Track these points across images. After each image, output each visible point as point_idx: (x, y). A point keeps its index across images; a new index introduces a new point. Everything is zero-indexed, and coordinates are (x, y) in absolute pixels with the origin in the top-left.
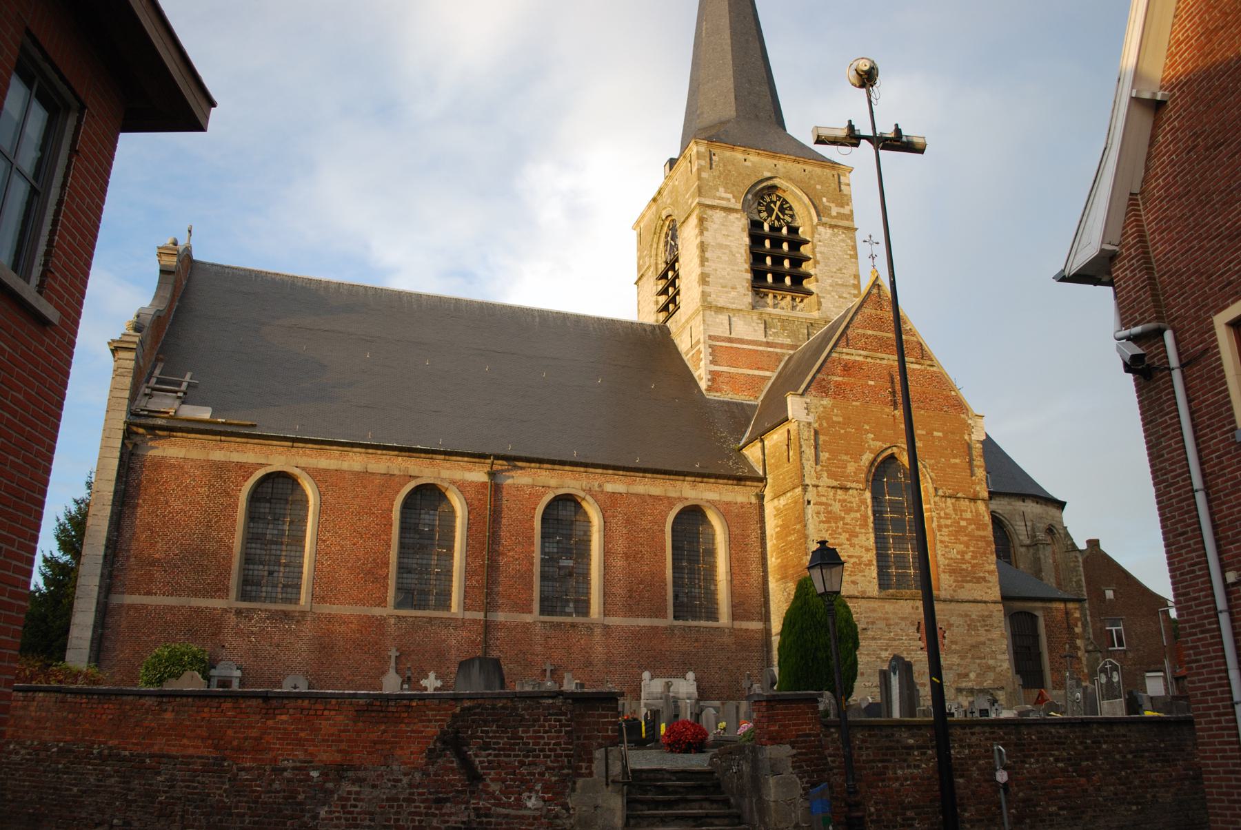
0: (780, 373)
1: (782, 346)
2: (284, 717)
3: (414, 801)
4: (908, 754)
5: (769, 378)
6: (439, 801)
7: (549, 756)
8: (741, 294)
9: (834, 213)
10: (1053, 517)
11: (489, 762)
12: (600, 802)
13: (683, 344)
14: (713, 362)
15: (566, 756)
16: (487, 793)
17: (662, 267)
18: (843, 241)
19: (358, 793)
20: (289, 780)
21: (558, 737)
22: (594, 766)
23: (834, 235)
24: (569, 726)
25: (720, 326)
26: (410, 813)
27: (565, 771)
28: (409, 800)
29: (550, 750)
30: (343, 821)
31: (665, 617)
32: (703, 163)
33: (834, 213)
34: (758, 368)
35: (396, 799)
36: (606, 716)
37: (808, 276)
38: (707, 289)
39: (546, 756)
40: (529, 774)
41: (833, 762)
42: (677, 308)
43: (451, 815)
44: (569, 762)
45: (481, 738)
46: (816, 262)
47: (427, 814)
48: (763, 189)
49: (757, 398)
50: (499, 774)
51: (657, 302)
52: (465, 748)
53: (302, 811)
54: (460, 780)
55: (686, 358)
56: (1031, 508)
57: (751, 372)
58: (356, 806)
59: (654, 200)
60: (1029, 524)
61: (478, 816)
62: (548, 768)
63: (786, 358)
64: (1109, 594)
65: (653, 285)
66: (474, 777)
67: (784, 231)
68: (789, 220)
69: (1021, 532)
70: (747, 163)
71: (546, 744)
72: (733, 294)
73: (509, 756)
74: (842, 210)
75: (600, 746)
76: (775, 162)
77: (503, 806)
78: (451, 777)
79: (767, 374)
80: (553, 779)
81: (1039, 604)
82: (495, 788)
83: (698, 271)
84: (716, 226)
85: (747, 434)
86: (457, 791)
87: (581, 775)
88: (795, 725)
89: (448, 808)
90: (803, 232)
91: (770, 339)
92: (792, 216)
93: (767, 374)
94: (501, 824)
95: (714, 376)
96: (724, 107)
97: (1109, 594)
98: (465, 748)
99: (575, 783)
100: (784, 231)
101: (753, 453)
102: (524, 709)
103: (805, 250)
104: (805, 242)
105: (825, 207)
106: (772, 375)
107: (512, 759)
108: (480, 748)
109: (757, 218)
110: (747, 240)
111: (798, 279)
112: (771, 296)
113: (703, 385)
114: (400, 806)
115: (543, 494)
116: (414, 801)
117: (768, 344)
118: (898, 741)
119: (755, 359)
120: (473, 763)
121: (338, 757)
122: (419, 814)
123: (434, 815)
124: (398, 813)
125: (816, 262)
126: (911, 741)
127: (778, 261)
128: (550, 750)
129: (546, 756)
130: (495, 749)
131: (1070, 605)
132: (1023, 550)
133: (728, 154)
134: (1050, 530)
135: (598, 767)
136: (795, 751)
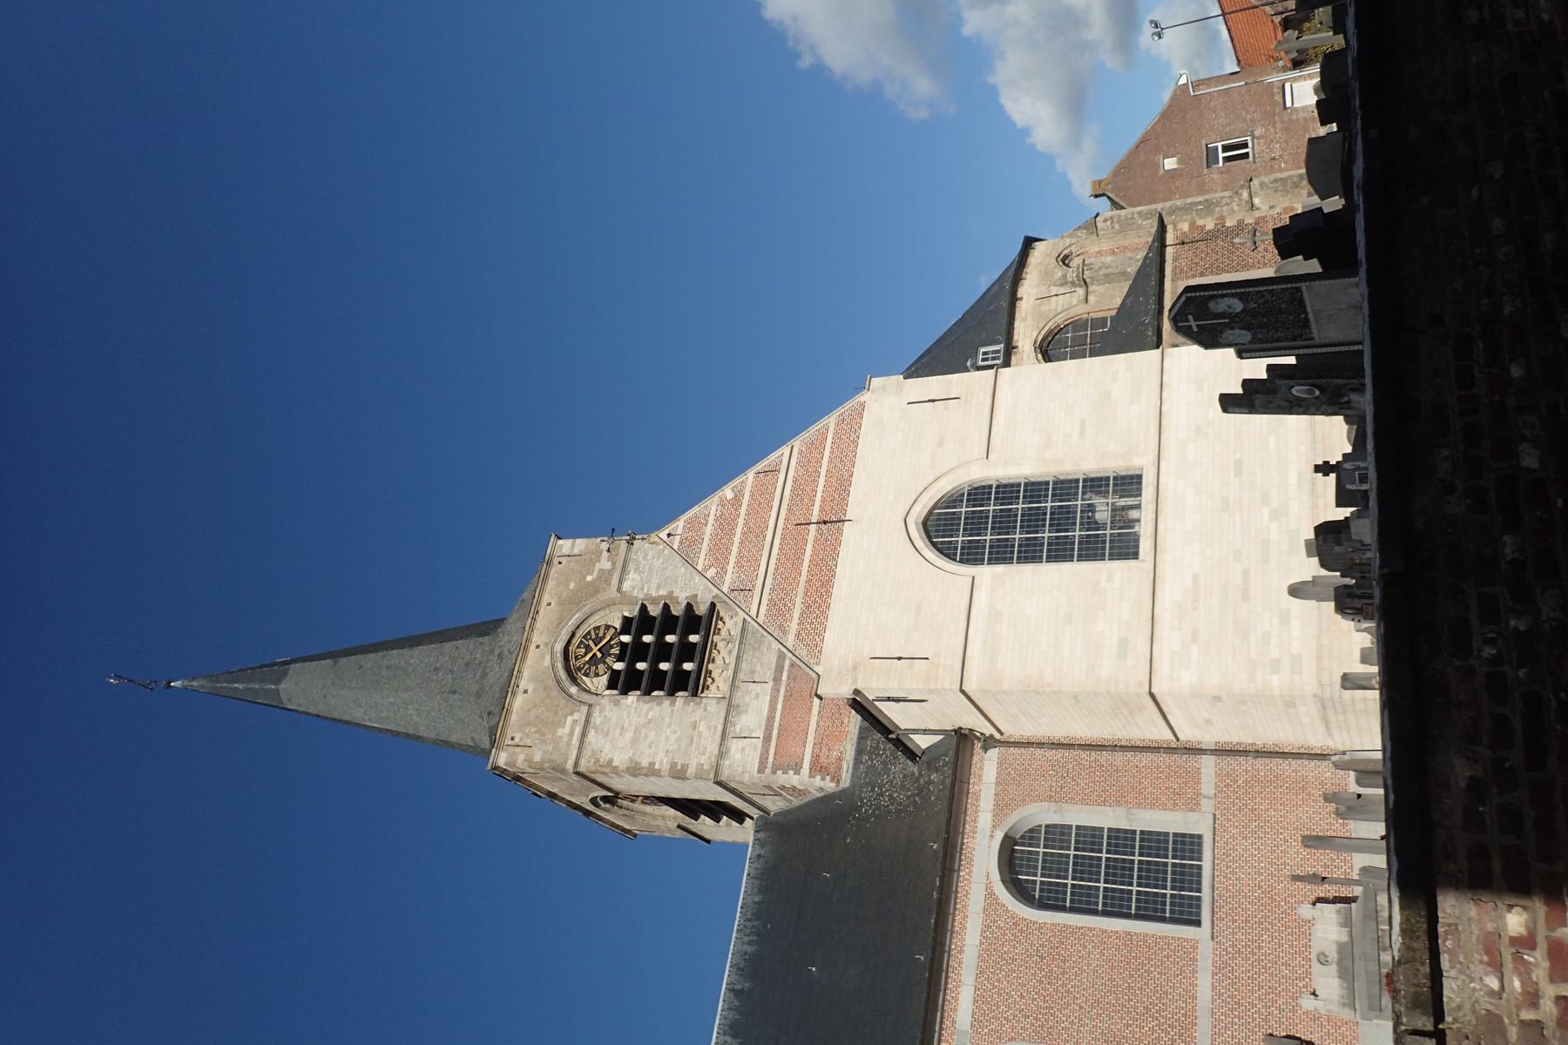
9: (608, 566)
33: (608, 566)
37: (689, 607)
60: (1054, 290)
64: (1170, 163)
67: (626, 639)
68: (612, 631)
72: (702, 727)
76: (532, 647)
90: (634, 612)
91: (769, 675)
92: (608, 627)
95: (818, 768)
97: (1170, 163)
100: (626, 639)
103: (654, 611)
104: (644, 608)
105: (599, 577)
110: (633, 697)
112: (711, 667)
113: (830, 786)
117: (777, 680)
127: (663, 651)
133: (514, 717)
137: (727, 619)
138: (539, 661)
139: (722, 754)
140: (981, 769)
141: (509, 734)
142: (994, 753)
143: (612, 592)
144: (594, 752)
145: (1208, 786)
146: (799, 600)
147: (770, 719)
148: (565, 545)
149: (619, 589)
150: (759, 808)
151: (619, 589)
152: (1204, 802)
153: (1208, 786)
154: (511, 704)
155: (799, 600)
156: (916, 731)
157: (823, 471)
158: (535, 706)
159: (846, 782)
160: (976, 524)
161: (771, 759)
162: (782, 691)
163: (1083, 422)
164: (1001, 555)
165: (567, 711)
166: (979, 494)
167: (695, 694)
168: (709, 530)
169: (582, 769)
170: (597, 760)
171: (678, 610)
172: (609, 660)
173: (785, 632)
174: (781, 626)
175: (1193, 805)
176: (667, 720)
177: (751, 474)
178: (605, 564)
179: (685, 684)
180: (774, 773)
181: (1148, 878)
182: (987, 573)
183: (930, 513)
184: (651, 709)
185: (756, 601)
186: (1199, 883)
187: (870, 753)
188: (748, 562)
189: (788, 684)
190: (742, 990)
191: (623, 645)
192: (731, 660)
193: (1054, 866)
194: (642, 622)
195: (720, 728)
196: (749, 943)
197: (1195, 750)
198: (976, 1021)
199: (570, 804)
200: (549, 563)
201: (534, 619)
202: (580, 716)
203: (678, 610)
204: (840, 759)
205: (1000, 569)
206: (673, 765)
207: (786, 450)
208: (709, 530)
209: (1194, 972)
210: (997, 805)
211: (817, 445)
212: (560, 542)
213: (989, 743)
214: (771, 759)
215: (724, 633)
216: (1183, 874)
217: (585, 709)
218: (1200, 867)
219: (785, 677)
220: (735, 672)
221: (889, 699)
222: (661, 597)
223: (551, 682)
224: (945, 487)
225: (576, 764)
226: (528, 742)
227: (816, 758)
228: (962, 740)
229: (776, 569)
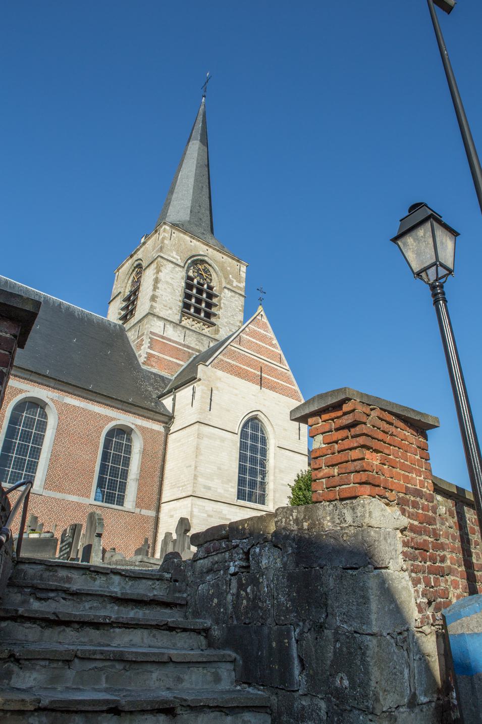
0: (189, 365)
1: (193, 349)
5: (182, 366)
8: (174, 313)
9: (234, 285)
13: (131, 336)
14: (150, 348)
17: (127, 293)
25: (157, 326)
31: (88, 497)
33: (234, 285)
34: (177, 358)
37: (215, 315)
38: (154, 304)
46: (220, 308)
48: (197, 260)
49: (172, 375)
51: (120, 314)
55: (132, 345)
63: (194, 356)
67: (205, 286)
68: (209, 281)
72: (170, 312)
74: (239, 285)
76: (207, 248)
83: (151, 294)
90: (215, 291)
91: (186, 343)
92: (211, 280)
95: (149, 356)
100: (205, 286)
101: (167, 402)
103: (215, 300)
104: (216, 296)
111: (208, 315)
112: (191, 319)
113: (141, 360)
119: (176, 352)
125: (220, 308)
127: (199, 301)
133: (182, 235)
137: (208, 329)
138: (201, 249)
139: (158, 317)
140: (157, 424)
141: (176, 232)
142: (162, 430)
143: (224, 285)
144: (165, 265)
146: (234, 363)
147: (170, 340)
148: (244, 269)
149: (225, 287)
150: (130, 329)
151: (225, 287)
152: (139, 510)
154: (187, 235)
155: (234, 363)
156: (174, 400)
158: (185, 245)
159: (144, 367)
160: (254, 438)
161: (155, 337)
162: (180, 347)
164: (243, 446)
165: (182, 257)
166: (264, 441)
168: (262, 331)
169: (159, 259)
170: (162, 266)
171: (214, 310)
172: (198, 278)
173: (223, 355)
174: (226, 354)
175: (138, 505)
176: (174, 298)
177: (280, 352)
178: (235, 284)
180: (150, 338)
181: (111, 483)
182: (237, 438)
183: (260, 421)
184: (179, 292)
185: (235, 345)
186: (108, 503)
187: (155, 379)
189: (182, 350)
190: (61, 308)
191: (202, 285)
192: (193, 328)
193: (118, 445)
195: (169, 319)
196: (78, 314)
197: (158, 510)
198: (67, 405)
199: (138, 250)
200: (238, 261)
201: (218, 251)
203: (214, 310)
204: (152, 366)
205: (239, 445)
206: (157, 297)
207: (288, 367)
208: (262, 331)
209: (79, 495)
210: (144, 428)
211: (288, 380)
212: (245, 267)
213: (167, 430)
214: (155, 337)
215: (204, 327)
216: (112, 497)
217: (182, 264)
218: (114, 504)
219: (185, 349)
220: (189, 329)
221: (194, 392)
222: (220, 304)
224: (269, 429)
225: (162, 257)
226: (172, 239)
227: (153, 356)
228: (168, 419)
229: (246, 356)
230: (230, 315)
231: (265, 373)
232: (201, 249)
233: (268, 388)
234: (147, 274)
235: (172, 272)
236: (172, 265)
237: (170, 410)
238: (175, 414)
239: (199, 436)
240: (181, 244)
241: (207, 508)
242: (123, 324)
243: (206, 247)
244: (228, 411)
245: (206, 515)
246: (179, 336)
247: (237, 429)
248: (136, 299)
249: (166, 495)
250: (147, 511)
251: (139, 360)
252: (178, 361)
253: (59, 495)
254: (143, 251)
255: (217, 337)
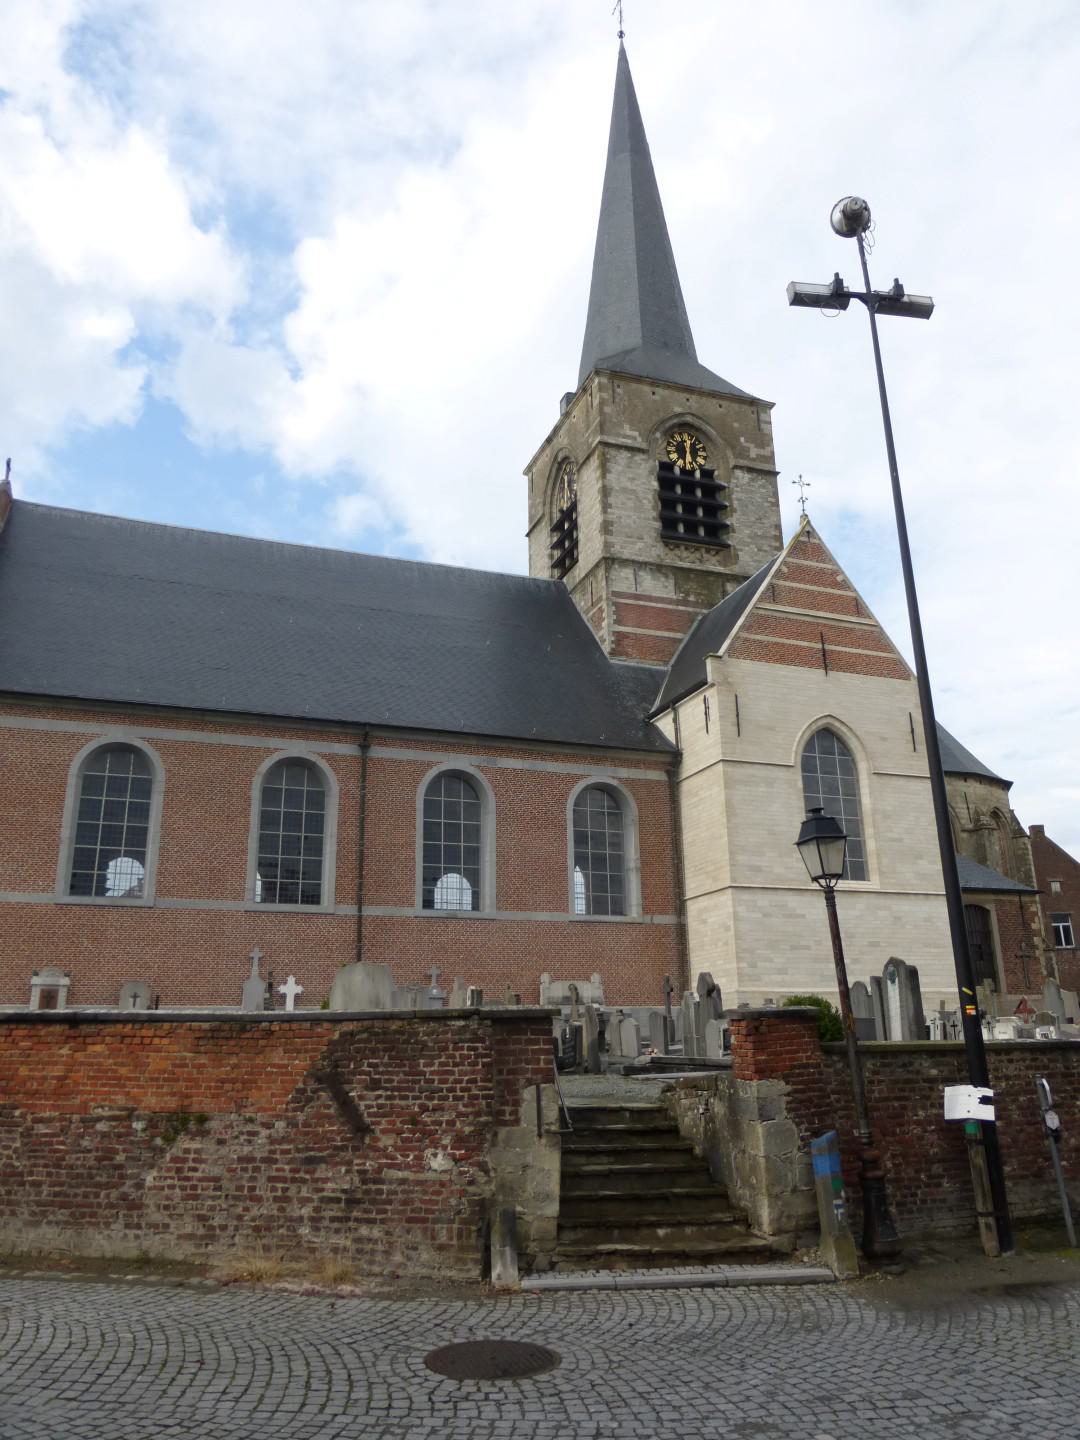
0: (693, 636)
2: (98, 1048)
3: (276, 1161)
4: (931, 1089)
5: (680, 640)
6: (310, 1161)
7: (461, 1098)
10: (998, 800)
11: (380, 1107)
12: (529, 1159)
13: (581, 602)
14: (618, 622)
15: (485, 1097)
16: (376, 1149)
17: (557, 516)
18: (763, 487)
19: (197, 1151)
20: (104, 1135)
21: (473, 1072)
22: (522, 1110)
23: (753, 480)
24: (486, 1056)
26: (271, 1179)
27: (483, 1119)
28: (269, 1160)
29: (462, 1090)
30: (177, 1190)
32: (605, 395)
34: (668, 630)
35: (250, 1159)
36: (537, 1042)
38: (611, 539)
39: (456, 1098)
40: (434, 1123)
41: (838, 1101)
42: (575, 561)
43: (326, 1180)
44: (488, 1105)
45: (368, 1074)
47: (293, 1180)
50: (393, 1123)
51: (551, 556)
52: (347, 1087)
53: (122, 1177)
54: (339, 1133)
55: (585, 618)
56: (974, 789)
57: (659, 633)
58: (195, 1170)
59: (549, 440)
61: (364, 1182)
62: (460, 1115)
63: (700, 618)
64: (1056, 887)
65: (545, 538)
66: (361, 1129)
67: (698, 474)
69: (962, 815)
70: (657, 397)
71: (457, 1081)
72: (640, 545)
73: (406, 1098)
74: (762, 452)
75: (529, 1082)
76: (688, 396)
77: (398, 1167)
78: (328, 1128)
79: (678, 635)
80: (467, 1129)
81: (992, 897)
82: (387, 1141)
83: (599, 519)
84: (620, 468)
85: (657, 703)
86: (336, 1148)
87: (505, 1123)
88: (788, 1052)
89: (322, 1171)
93: (678, 635)
94: (395, 1193)
95: (620, 638)
96: (629, 336)
97: (1056, 887)
98: (347, 1087)
99: (495, 1134)
100: (698, 474)
101: (665, 724)
102: (428, 1035)
106: (684, 637)
107: (411, 1102)
108: (367, 1088)
109: (665, 459)
110: (655, 484)
112: (682, 548)
113: (606, 648)
114: (256, 1169)
115: (423, 772)
116: (276, 1161)
118: (918, 1072)
119: (664, 618)
120: (356, 1108)
121: (172, 1103)
122: (284, 1180)
123: (304, 1181)
124: (253, 1179)
125: (734, 510)
126: (934, 1072)
127: (690, 508)
128: (462, 1090)
129: (456, 1098)
130: (386, 1089)
131: (1025, 899)
132: (965, 835)
134: (996, 814)
135: (528, 1110)
136: (789, 1088)
141: (622, 383)
145: (659, 919)
147: (650, 598)
149: (736, 467)
153: (659, 919)
156: (675, 720)
157: (859, 651)
159: (613, 661)
163: (900, 840)
167: (663, 537)
179: (669, 529)
182: (797, 778)
188: (795, 598)
191: (692, 472)
194: (712, 489)
197: (680, 909)
198: (503, 771)
202: (640, 443)
204: (627, 654)
205: (800, 784)
206: (612, 524)
219: (681, 608)
223: (662, 415)
226: (617, 400)
228: (672, 758)
229: (789, 620)
230: (753, 519)
231: (832, 642)
232: (679, 405)
233: (841, 669)
234: (585, 478)
235: (629, 467)
236: (625, 454)
237: (674, 742)
238: (685, 746)
239: (729, 784)
240: (636, 406)
241: (759, 903)
242: (561, 577)
243: (683, 396)
244: (772, 729)
245: (760, 915)
246: (666, 587)
247: (794, 757)
248: (574, 526)
249: (691, 887)
250: (660, 917)
251: (603, 647)
252: (671, 635)
253: (520, 916)
254: (569, 430)
255: (736, 569)
